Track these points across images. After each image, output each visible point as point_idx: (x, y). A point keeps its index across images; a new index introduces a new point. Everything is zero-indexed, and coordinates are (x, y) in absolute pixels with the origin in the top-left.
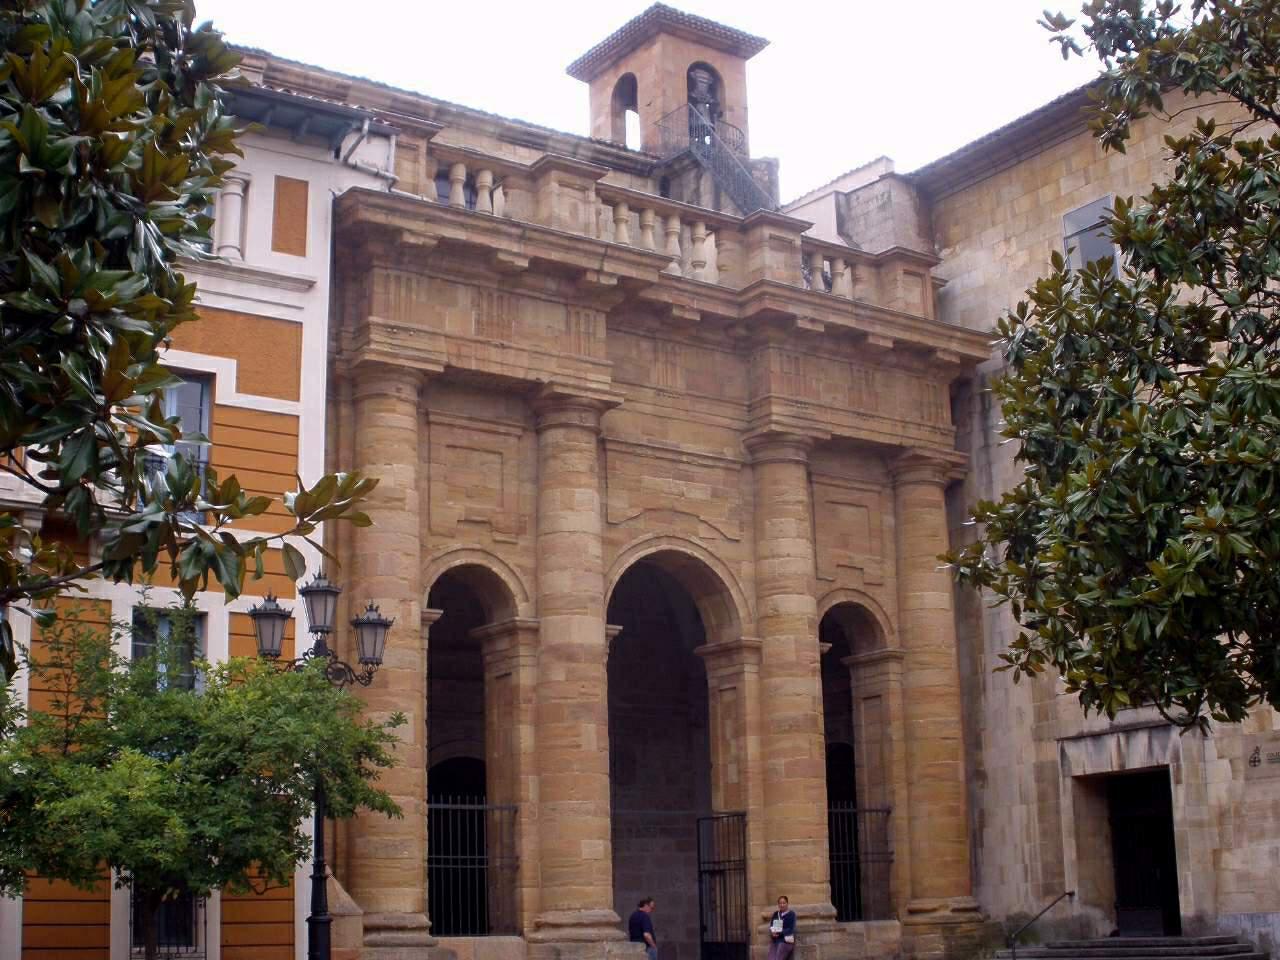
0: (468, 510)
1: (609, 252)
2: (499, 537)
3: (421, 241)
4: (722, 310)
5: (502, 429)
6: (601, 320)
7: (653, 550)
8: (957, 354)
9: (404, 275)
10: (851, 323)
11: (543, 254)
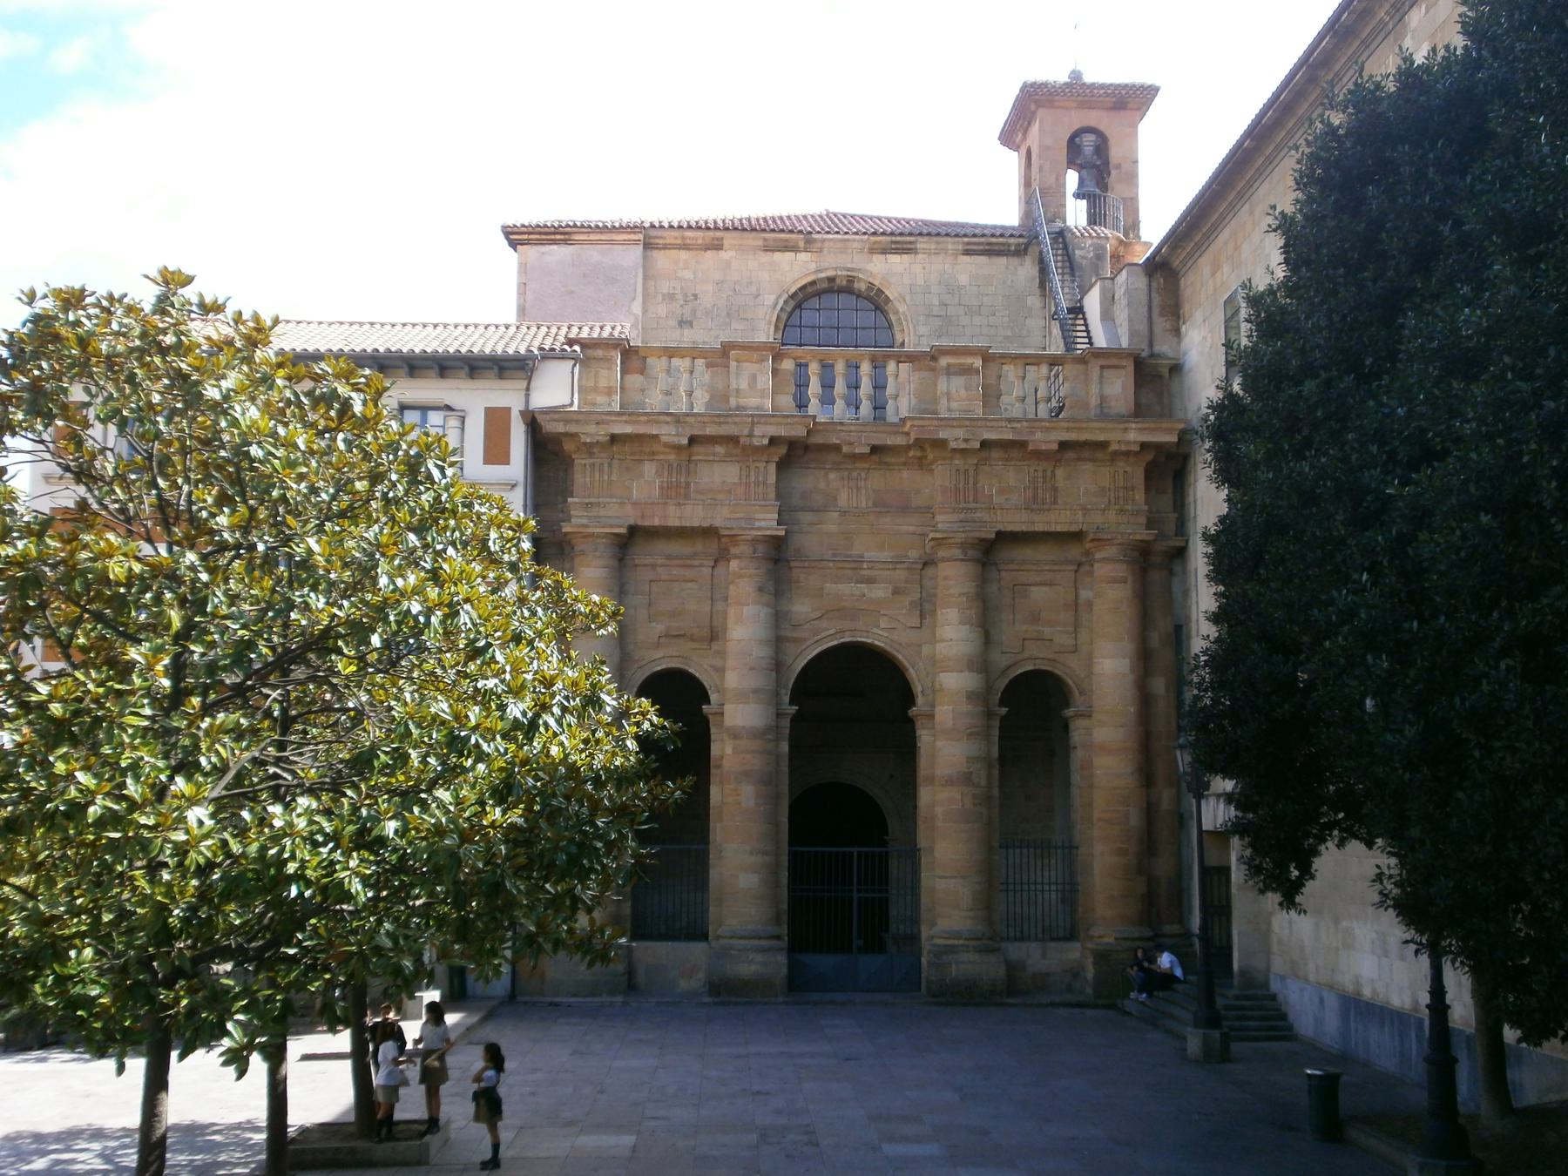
2: (696, 645)
5: (696, 563)
6: (772, 468)
7: (835, 643)
8: (1135, 442)
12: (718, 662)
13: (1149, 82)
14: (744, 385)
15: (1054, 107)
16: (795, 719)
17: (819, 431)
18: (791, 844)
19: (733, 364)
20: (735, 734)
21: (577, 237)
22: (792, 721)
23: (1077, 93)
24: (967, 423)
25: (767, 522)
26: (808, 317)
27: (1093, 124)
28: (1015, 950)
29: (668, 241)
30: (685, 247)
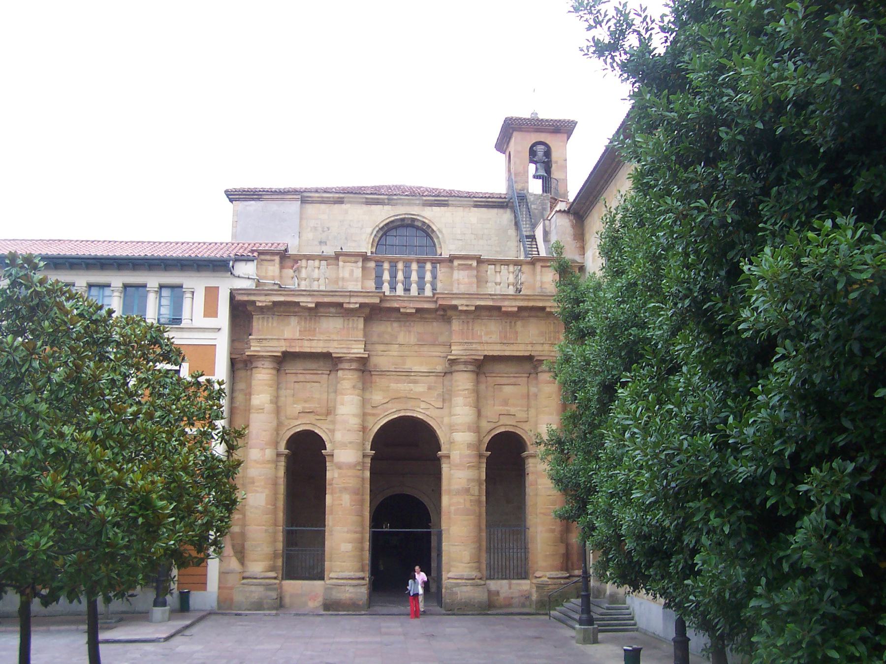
0: (304, 408)
1: (352, 294)
2: (318, 417)
3: (264, 304)
4: (426, 306)
5: (320, 372)
6: (361, 320)
7: (396, 416)
9: (266, 316)
10: (490, 303)
11: (321, 300)
12: (331, 427)
13: (572, 119)
14: (347, 275)
15: (522, 131)
16: (373, 459)
17: (387, 300)
18: (372, 527)
19: (341, 263)
20: (339, 467)
21: (264, 197)
22: (371, 459)
23: (535, 125)
24: (467, 296)
25: (358, 350)
26: (390, 240)
27: (542, 140)
28: (494, 585)
29: (314, 199)
30: (323, 202)
